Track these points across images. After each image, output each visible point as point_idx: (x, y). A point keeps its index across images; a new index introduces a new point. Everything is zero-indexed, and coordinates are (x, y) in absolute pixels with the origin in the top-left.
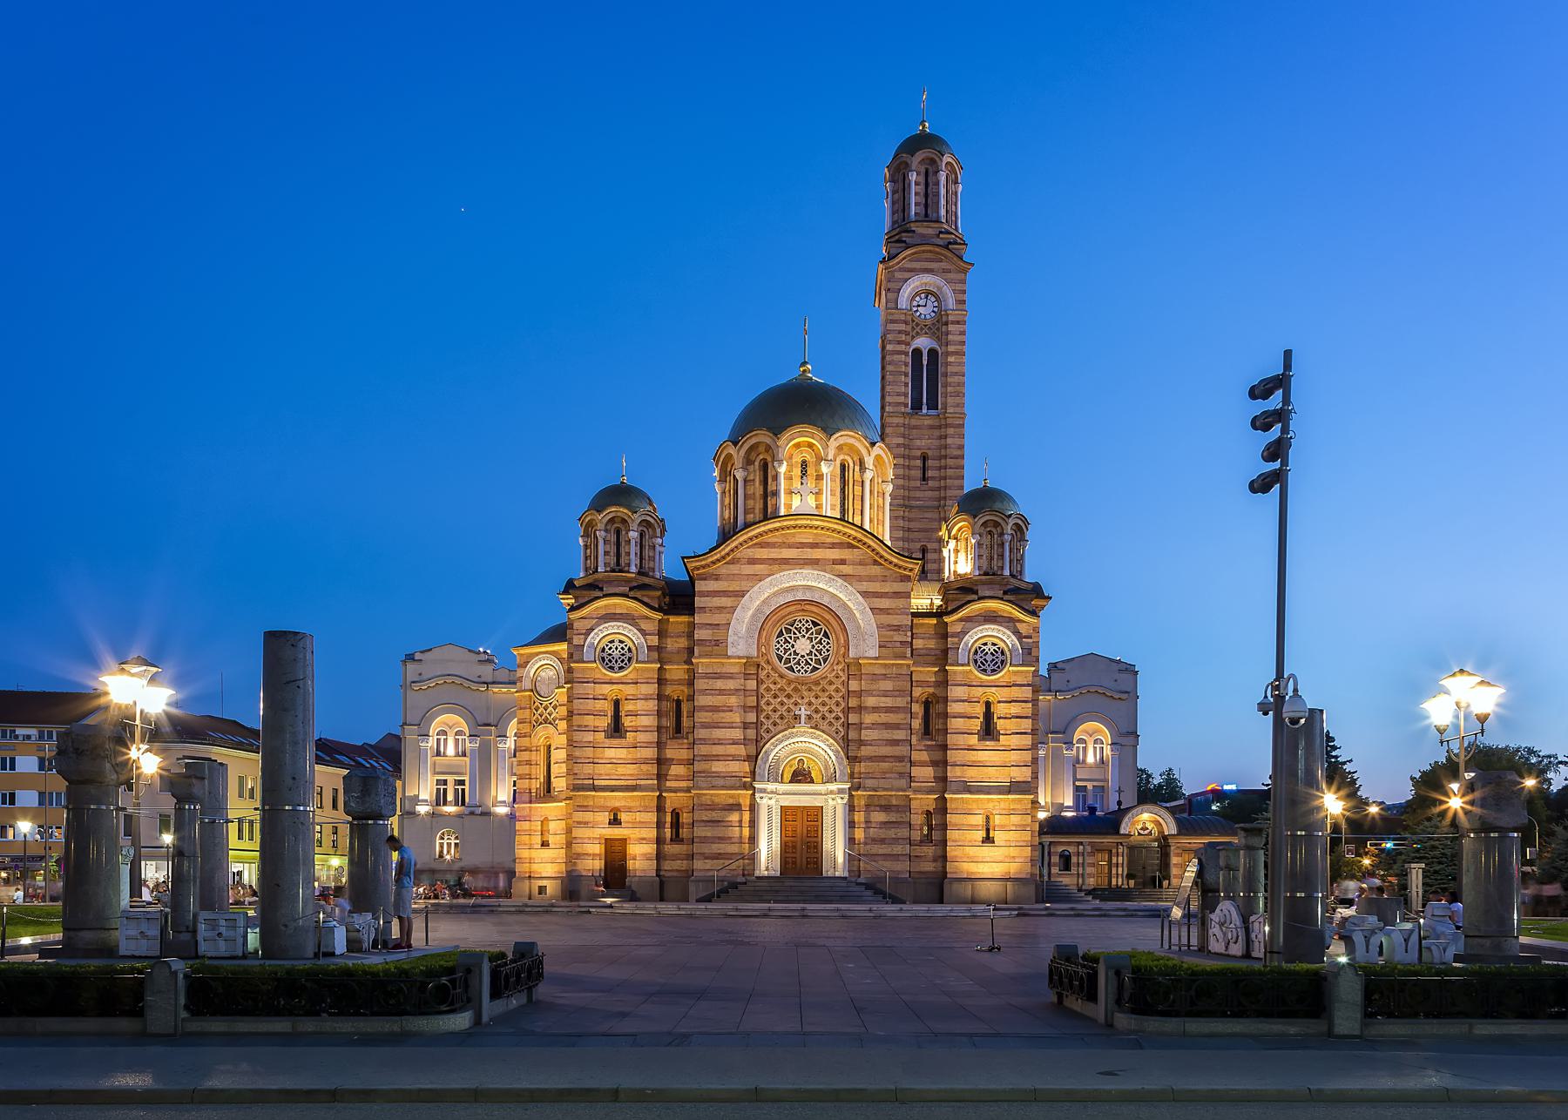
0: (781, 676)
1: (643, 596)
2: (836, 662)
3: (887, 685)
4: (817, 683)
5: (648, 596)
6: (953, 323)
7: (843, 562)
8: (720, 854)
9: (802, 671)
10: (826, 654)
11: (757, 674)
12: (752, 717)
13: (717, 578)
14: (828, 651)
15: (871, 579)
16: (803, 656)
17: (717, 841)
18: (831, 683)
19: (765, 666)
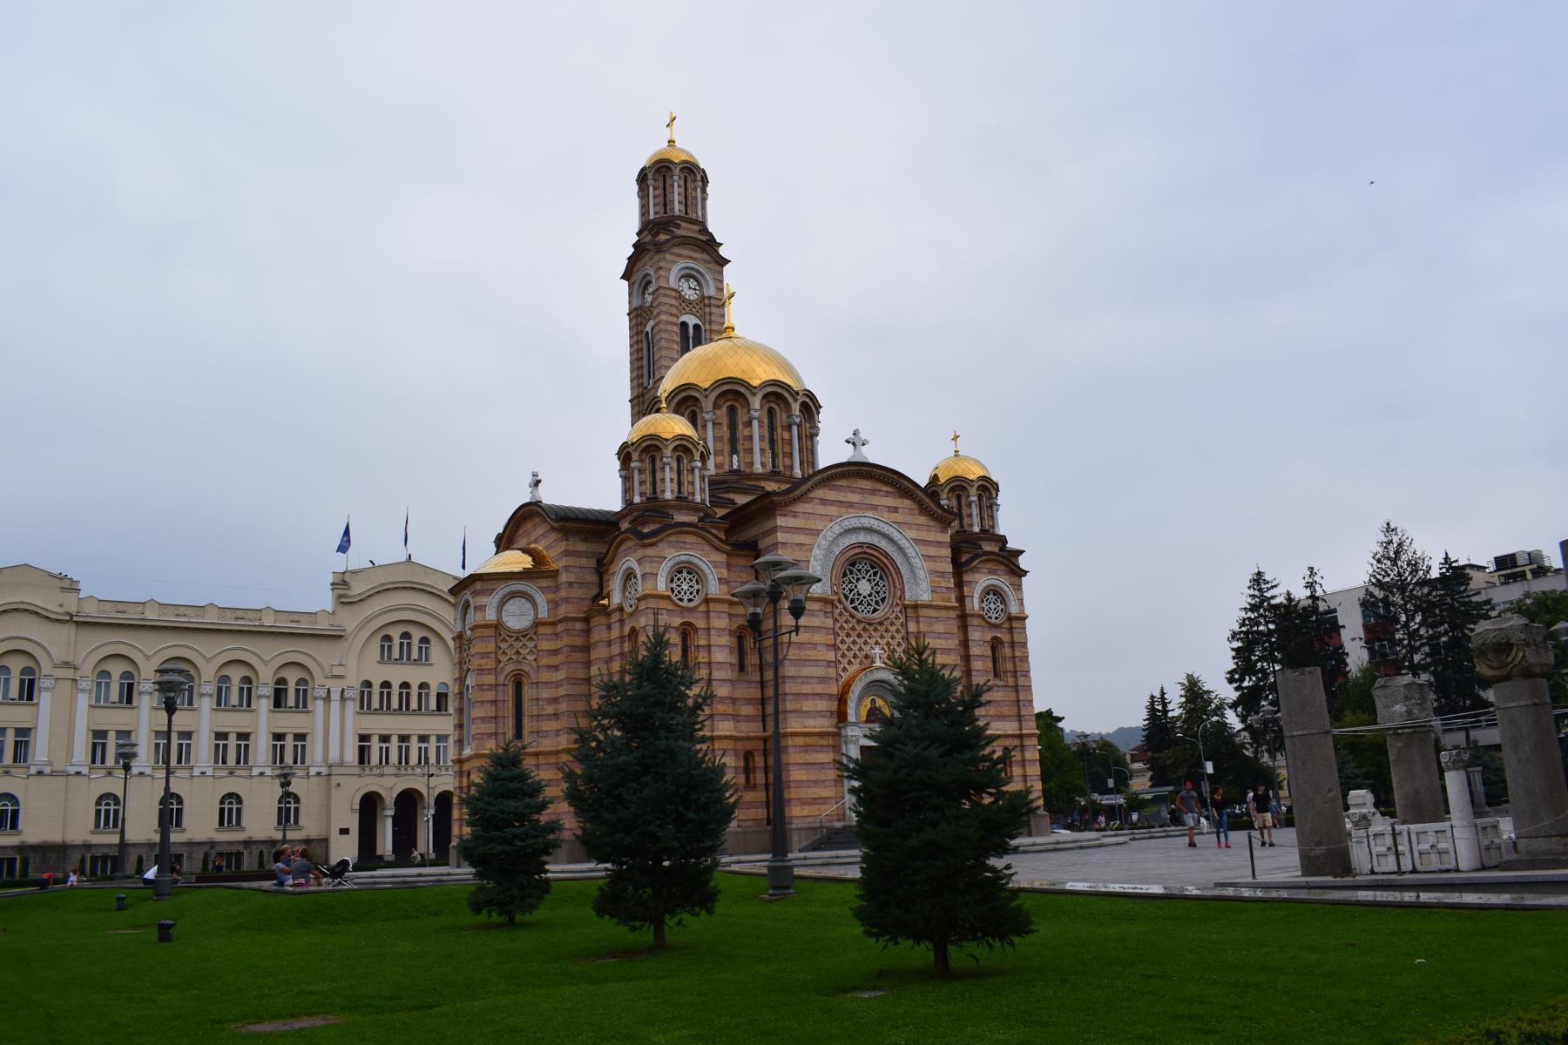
0: (852, 616)
1: (712, 527)
2: (895, 604)
3: (939, 628)
4: (881, 624)
5: (716, 528)
6: (714, 306)
7: (895, 510)
8: (815, 799)
9: (866, 611)
10: (884, 596)
11: (832, 613)
12: (831, 656)
13: (795, 514)
14: (885, 593)
15: (919, 527)
16: (865, 597)
17: (811, 784)
18: (892, 624)
19: (838, 605)
